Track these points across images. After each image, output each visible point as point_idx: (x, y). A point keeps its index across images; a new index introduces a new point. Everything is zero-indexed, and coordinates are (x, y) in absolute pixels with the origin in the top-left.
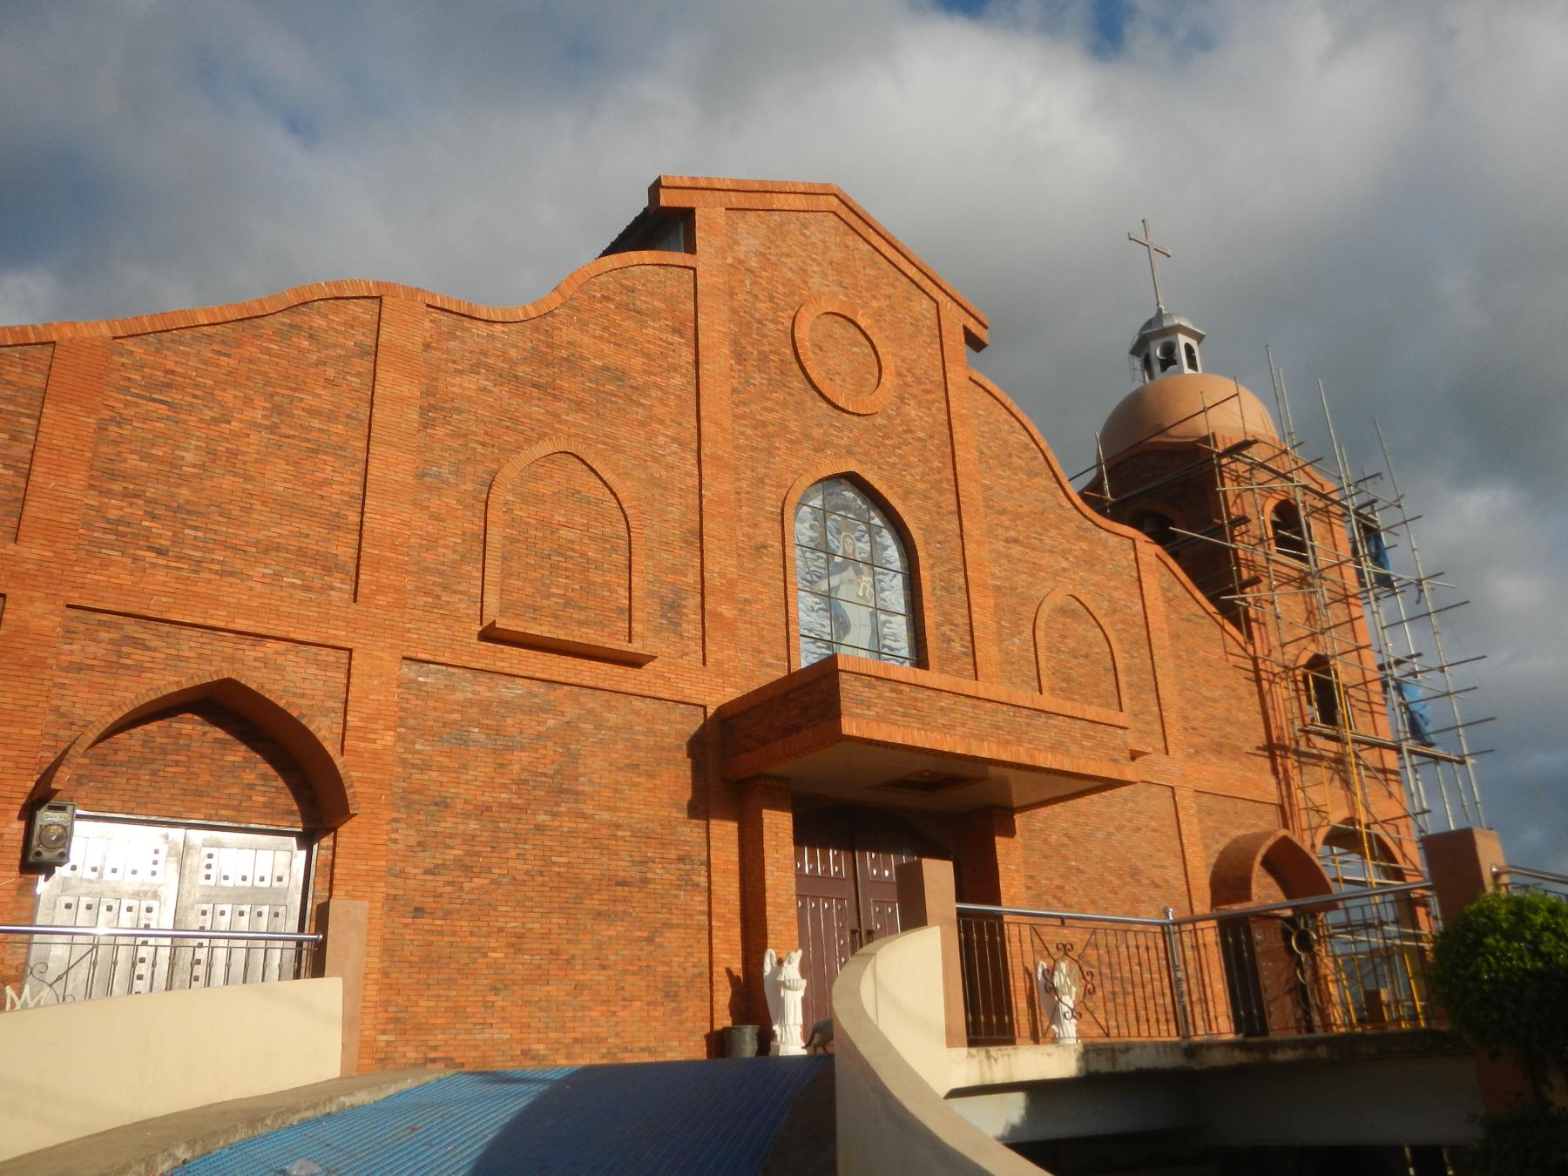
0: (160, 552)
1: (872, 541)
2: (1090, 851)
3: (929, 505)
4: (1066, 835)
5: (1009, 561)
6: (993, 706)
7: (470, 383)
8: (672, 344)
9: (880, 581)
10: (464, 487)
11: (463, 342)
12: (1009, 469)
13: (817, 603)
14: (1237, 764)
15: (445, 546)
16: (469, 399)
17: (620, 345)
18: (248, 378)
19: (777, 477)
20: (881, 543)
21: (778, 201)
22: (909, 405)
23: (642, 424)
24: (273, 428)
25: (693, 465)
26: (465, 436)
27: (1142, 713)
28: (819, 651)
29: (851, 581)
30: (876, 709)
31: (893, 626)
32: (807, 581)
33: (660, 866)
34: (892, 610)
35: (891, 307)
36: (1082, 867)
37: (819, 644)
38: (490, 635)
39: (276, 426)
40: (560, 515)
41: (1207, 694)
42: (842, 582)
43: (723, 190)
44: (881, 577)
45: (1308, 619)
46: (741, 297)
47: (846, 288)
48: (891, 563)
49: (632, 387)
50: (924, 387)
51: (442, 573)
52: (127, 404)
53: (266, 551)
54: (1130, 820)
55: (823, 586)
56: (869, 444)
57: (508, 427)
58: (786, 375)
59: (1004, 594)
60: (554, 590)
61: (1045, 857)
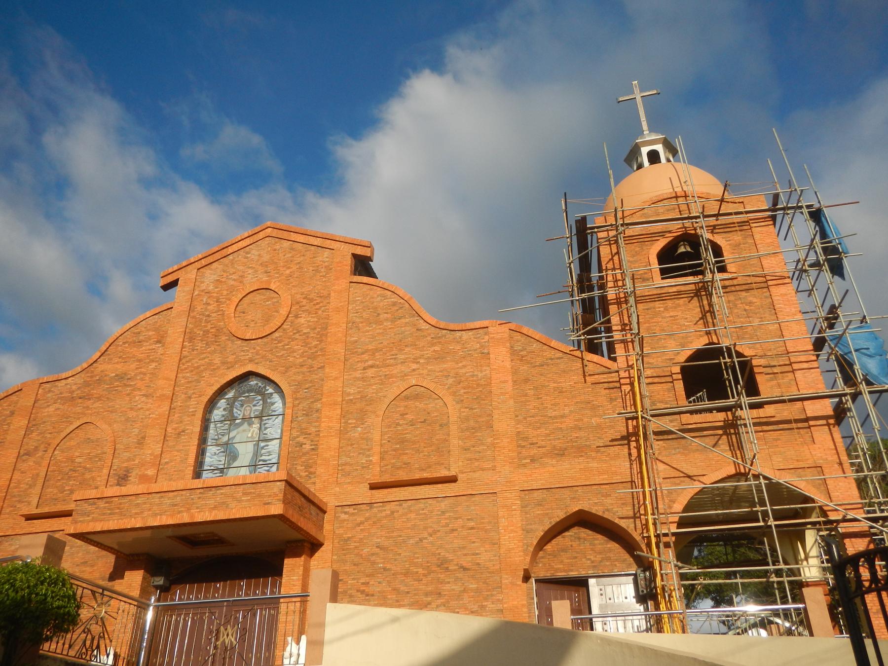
1: (265, 402)
3: (304, 369)
4: (377, 547)
5: (364, 381)
6: (175, 493)
7: (51, 409)
8: (154, 349)
10: (38, 455)
11: (54, 392)
13: (218, 450)
15: (23, 484)
16: (49, 416)
19: (200, 392)
21: (230, 250)
23: (128, 395)
25: (152, 404)
27: (474, 447)
28: (214, 476)
29: (244, 431)
30: (93, 515)
31: (269, 447)
32: (214, 440)
33: (86, 610)
35: (301, 268)
36: (388, 566)
37: (216, 472)
38: (29, 518)
40: (79, 452)
42: (238, 433)
44: (267, 421)
45: (703, 317)
46: (199, 308)
47: (269, 272)
48: (275, 411)
50: (315, 302)
51: (19, 496)
54: (447, 525)
55: (225, 439)
56: (266, 351)
57: (63, 422)
59: (355, 403)
60: (67, 488)
61: (355, 565)
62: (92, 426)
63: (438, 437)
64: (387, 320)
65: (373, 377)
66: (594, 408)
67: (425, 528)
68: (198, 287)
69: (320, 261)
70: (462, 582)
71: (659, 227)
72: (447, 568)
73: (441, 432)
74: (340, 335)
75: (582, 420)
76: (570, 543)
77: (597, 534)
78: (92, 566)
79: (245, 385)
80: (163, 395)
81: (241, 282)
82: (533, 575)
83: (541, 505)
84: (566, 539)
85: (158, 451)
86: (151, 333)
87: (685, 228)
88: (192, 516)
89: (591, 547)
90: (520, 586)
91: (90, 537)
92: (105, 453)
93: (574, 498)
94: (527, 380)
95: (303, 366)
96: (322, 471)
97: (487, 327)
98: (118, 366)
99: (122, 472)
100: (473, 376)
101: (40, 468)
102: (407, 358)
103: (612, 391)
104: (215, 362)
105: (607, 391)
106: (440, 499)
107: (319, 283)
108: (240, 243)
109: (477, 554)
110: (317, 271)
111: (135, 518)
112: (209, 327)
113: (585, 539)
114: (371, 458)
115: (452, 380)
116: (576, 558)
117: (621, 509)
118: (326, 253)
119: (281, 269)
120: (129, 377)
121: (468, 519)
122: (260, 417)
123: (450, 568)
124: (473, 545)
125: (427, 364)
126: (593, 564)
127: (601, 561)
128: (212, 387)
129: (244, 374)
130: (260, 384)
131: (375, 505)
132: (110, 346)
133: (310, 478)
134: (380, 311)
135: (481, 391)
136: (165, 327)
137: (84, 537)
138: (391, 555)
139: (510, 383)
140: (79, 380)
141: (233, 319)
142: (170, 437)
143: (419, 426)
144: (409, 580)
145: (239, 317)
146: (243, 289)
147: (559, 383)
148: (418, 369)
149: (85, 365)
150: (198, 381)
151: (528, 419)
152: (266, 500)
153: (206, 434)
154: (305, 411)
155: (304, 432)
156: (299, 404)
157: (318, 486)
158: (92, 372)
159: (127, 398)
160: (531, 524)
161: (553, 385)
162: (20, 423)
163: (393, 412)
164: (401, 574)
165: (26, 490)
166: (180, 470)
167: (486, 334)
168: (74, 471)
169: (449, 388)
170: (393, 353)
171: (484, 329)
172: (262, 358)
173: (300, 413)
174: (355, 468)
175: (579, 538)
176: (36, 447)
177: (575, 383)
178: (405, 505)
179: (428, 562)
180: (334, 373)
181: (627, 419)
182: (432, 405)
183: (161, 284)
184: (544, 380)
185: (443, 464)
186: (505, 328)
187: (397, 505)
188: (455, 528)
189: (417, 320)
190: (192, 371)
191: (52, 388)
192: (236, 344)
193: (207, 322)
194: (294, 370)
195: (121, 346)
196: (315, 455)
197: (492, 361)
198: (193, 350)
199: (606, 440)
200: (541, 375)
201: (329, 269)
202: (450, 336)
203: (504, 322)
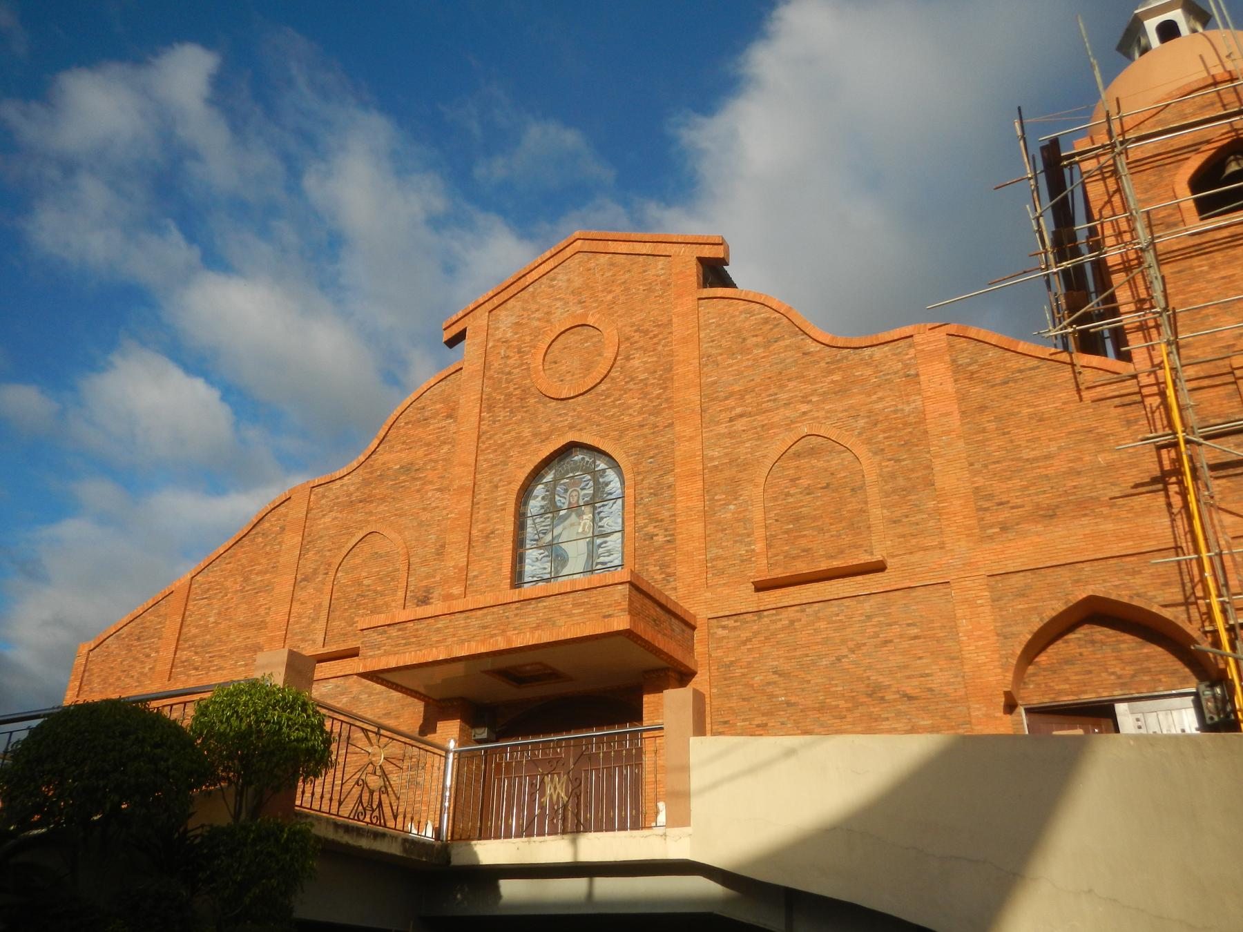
0: (196, 669)
1: (596, 482)
2: (809, 682)
3: (646, 431)
4: (775, 673)
6: (485, 611)
7: (327, 519)
9: (599, 513)
11: (327, 497)
12: (741, 354)
13: (540, 554)
14: (1085, 521)
16: (327, 528)
17: (411, 448)
18: (237, 570)
20: (604, 482)
21: (529, 279)
22: (634, 358)
24: (241, 591)
25: (449, 500)
26: (322, 550)
29: (572, 525)
34: (609, 531)
35: (627, 289)
36: (793, 699)
37: (540, 584)
39: (244, 588)
41: (1032, 454)
42: (564, 529)
43: (487, 301)
44: (602, 509)
46: (496, 365)
48: (611, 494)
49: (417, 470)
50: (651, 335)
51: (302, 633)
52: (194, 605)
53: (233, 653)
54: (876, 635)
55: (548, 538)
57: (344, 534)
58: (525, 398)
61: (744, 700)
62: (377, 537)
63: (849, 507)
64: (757, 345)
65: (744, 431)
66: (1100, 439)
67: (844, 642)
68: (492, 336)
69: (653, 276)
70: (908, 717)
71: (1187, 136)
72: (882, 698)
73: (854, 500)
74: (691, 376)
75: (1081, 459)
76: (1078, 651)
77: (1123, 634)
78: (398, 717)
79: (568, 463)
80: (462, 487)
81: (548, 321)
82: (1020, 702)
83: (1023, 595)
84: (1072, 644)
85: (463, 562)
86: (438, 406)
87: (1236, 130)
88: (509, 640)
89: (1114, 654)
90: (1000, 718)
91: (386, 676)
92: (398, 570)
93: (1078, 581)
94: (982, 409)
95: (643, 426)
96: (684, 570)
97: (912, 336)
98: (403, 455)
99: (421, 594)
100: (895, 412)
101: (321, 596)
102: (792, 397)
103: (1128, 408)
104: (525, 434)
105: (1120, 410)
106: (861, 598)
107: (654, 306)
108: (541, 267)
109: (928, 675)
110: (650, 290)
111: (437, 648)
112: (511, 389)
113: (1103, 643)
114: (753, 547)
115: (863, 421)
116: (1090, 672)
117: (1161, 592)
118: (662, 262)
119: (600, 295)
120: (417, 467)
121: (909, 625)
122: (591, 504)
123: (887, 698)
124: (918, 662)
125: (823, 401)
126: (1121, 681)
127: (1133, 676)
128: (522, 470)
129: (563, 446)
130: (587, 459)
131: (765, 613)
132: (389, 429)
133: (669, 582)
134: (745, 334)
135: (911, 433)
136: (455, 395)
137: (378, 678)
138: (796, 684)
139: (957, 415)
140: (355, 478)
141: (542, 373)
142: (477, 541)
143: (819, 494)
144: (826, 719)
145: (549, 369)
146: (551, 331)
147: (1037, 406)
148: (811, 411)
149: (362, 458)
150: (505, 463)
151: (990, 467)
152: (606, 611)
153: (523, 533)
154: (652, 488)
155: (654, 519)
156: (643, 480)
157: (682, 591)
158: (372, 466)
159: (418, 496)
160: (1010, 625)
161: (1026, 411)
162: (292, 540)
163: (779, 478)
164: (814, 709)
165: (309, 625)
166: (494, 585)
167: (910, 346)
168: (363, 596)
169: (860, 434)
170: (770, 392)
171: (908, 340)
172: (586, 421)
173: (646, 493)
174: (730, 563)
175: (1093, 642)
176: (315, 569)
177: (1064, 403)
178: (809, 610)
179: (852, 691)
180: (688, 432)
181: (1159, 448)
182: (836, 462)
183: (445, 339)
184: (1012, 405)
185: (861, 546)
186: (940, 334)
187: (797, 611)
188: (887, 639)
189: (802, 339)
190: (496, 451)
191: (325, 491)
192: (550, 407)
193: (508, 382)
194: (631, 434)
195: (403, 428)
196: (672, 549)
197: (924, 386)
198: (494, 422)
199: (1126, 485)
200: (1006, 397)
201: (666, 284)
202: (854, 356)
203: (938, 324)
